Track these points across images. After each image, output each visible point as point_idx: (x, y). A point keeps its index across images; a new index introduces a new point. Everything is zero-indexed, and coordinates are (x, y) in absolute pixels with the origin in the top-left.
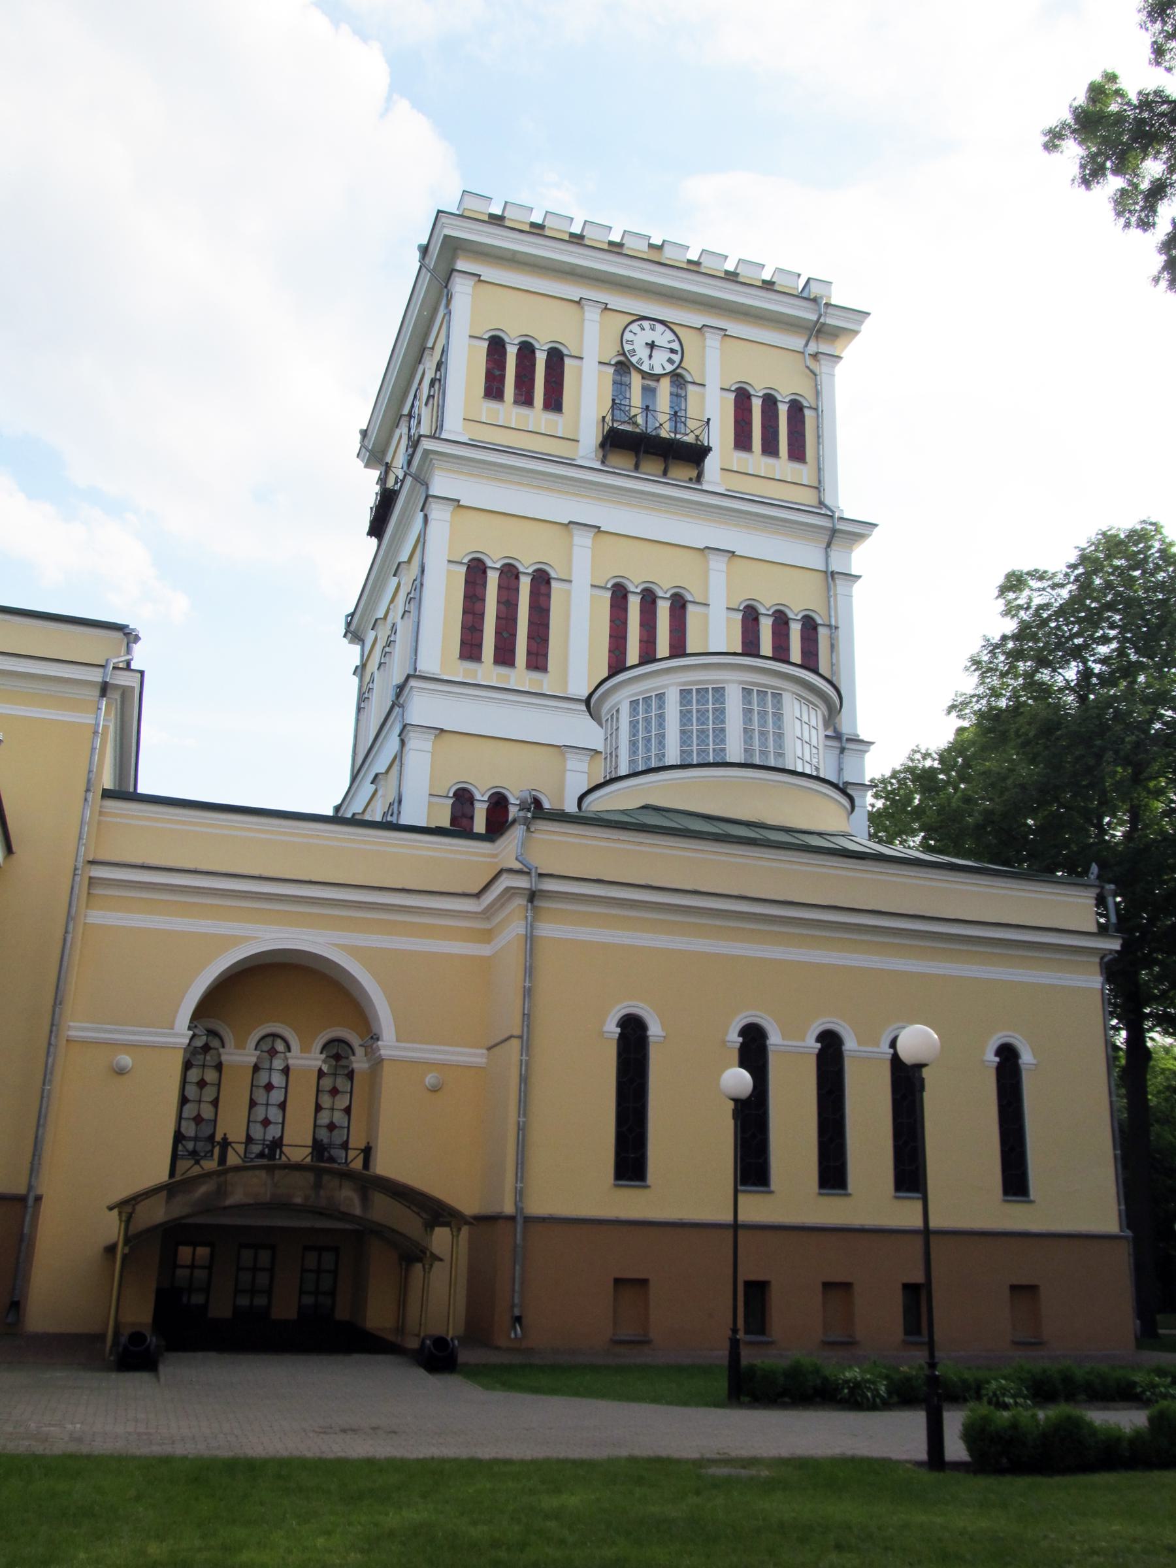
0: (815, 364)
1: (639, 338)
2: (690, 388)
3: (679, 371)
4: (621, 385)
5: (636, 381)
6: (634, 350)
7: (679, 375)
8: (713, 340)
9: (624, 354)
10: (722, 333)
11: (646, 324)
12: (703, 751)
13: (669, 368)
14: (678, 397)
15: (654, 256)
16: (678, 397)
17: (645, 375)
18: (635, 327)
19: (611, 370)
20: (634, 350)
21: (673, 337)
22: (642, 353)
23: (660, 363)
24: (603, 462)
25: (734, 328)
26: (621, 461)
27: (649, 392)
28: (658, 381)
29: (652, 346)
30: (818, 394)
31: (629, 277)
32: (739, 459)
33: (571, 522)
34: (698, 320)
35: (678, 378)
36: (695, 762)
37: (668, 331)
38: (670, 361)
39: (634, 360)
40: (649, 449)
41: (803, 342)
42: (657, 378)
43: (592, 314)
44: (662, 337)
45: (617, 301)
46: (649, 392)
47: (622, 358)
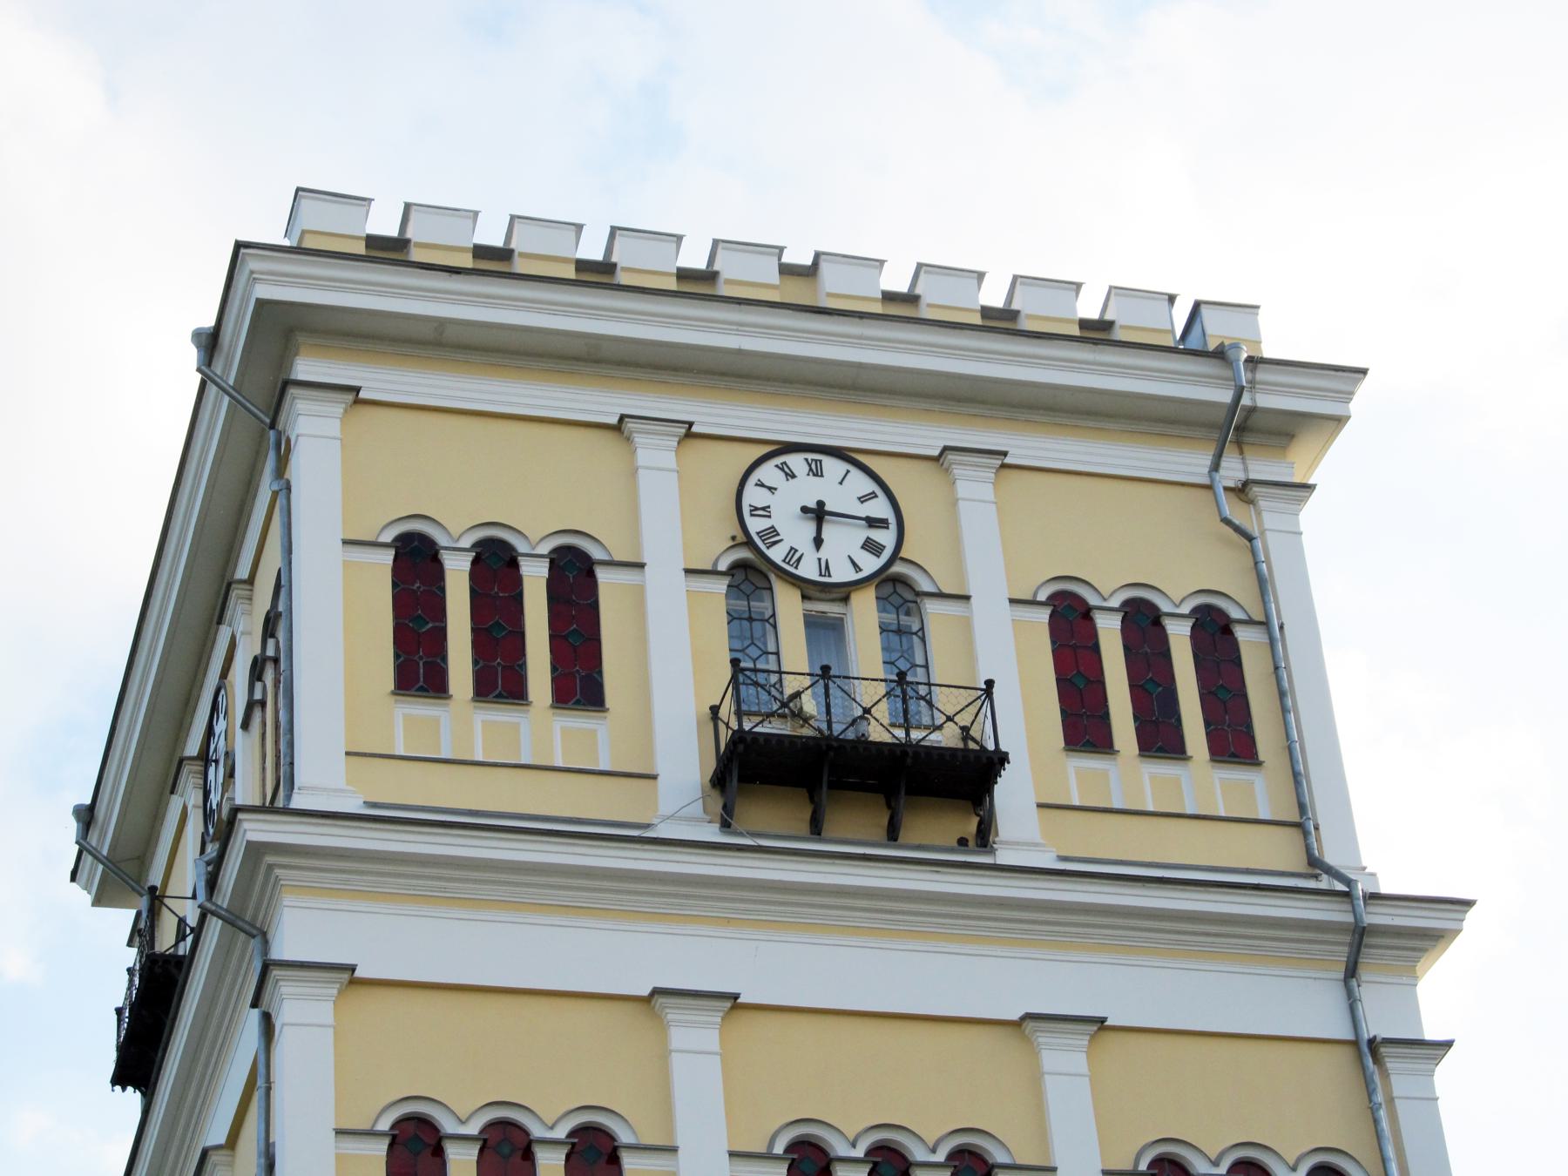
0: (1244, 514)
1: (783, 499)
2: (931, 607)
3: (898, 568)
6: (773, 531)
7: (900, 581)
11: (796, 461)
13: (871, 564)
15: (796, 292)
16: (902, 634)
17: (809, 590)
18: (769, 472)
19: (720, 586)
20: (773, 531)
21: (869, 486)
22: (797, 534)
23: (844, 557)
24: (726, 825)
25: (1025, 446)
26: (777, 815)
27: (826, 631)
28: (845, 599)
29: (818, 514)
30: (1263, 584)
31: (740, 352)
32: (1081, 776)
33: (656, 992)
34: (928, 436)
35: (895, 588)
37: (856, 475)
38: (871, 547)
39: (777, 554)
40: (844, 777)
41: (1206, 460)
42: (843, 592)
43: (656, 455)
46: (826, 631)
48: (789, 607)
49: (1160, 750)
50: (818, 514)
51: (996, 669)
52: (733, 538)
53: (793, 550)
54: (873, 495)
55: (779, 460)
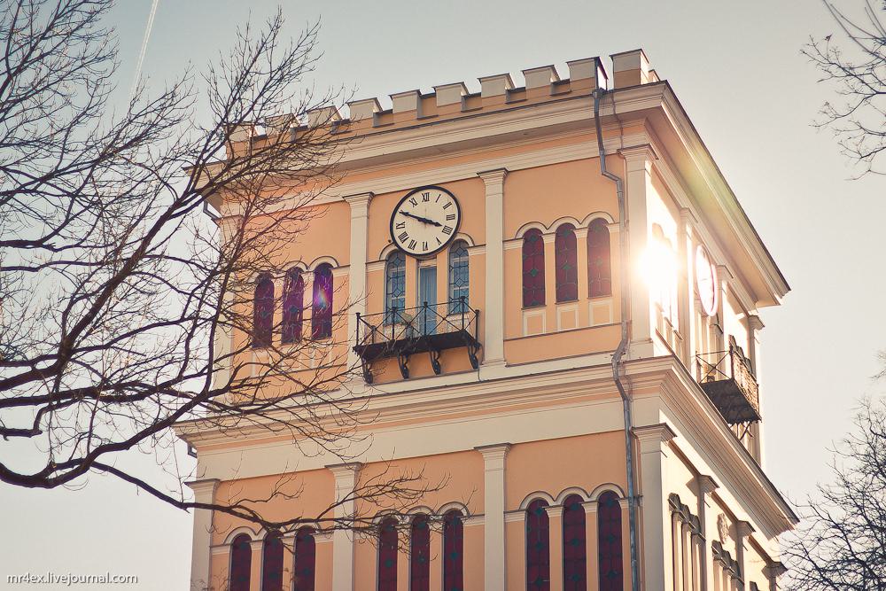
2: (471, 252)
3: (458, 237)
4: (395, 280)
5: (410, 267)
6: (405, 234)
8: (494, 186)
11: (418, 197)
13: (445, 238)
14: (459, 272)
19: (382, 266)
20: (405, 234)
25: (513, 161)
26: (392, 368)
27: (427, 275)
34: (468, 169)
37: (443, 194)
39: (405, 246)
40: (423, 348)
43: (359, 209)
44: (436, 207)
45: (380, 185)
46: (427, 275)
52: (390, 241)
54: (450, 204)
55: (410, 199)
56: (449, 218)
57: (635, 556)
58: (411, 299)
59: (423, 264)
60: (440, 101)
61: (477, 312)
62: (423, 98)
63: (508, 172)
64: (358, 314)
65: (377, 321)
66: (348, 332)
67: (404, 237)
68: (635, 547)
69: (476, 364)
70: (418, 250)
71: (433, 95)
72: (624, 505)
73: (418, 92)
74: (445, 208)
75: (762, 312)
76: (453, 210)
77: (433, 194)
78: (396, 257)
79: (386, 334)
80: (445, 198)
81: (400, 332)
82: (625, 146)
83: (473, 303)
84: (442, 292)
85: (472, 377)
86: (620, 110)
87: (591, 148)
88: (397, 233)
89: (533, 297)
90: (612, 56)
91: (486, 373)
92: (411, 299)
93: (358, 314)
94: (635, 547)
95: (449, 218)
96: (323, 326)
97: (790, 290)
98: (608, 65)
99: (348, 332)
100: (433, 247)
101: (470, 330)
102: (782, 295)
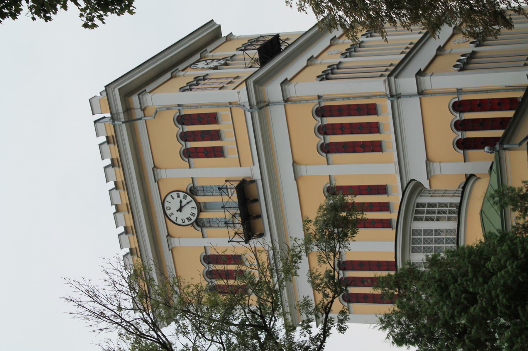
1: (179, 217)
3: (188, 191)
5: (204, 215)
6: (188, 219)
8: (162, 174)
9: (192, 224)
10: (155, 169)
11: (168, 212)
12: (446, 240)
13: (189, 198)
14: (205, 191)
17: (200, 211)
18: (173, 218)
19: (205, 230)
20: (188, 219)
31: (147, 230)
35: (193, 192)
36: (456, 237)
37: (167, 199)
38: (185, 198)
39: (194, 218)
43: (176, 242)
44: (173, 204)
45: (163, 233)
47: (195, 224)
48: (204, 215)
49: (215, 118)
50: (180, 210)
51: (209, 172)
53: (191, 215)
56: (178, 196)
57: (348, 98)
58: (219, 215)
59: (203, 210)
60: (119, 202)
61: (226, 181)
62: (118, 210)
63: (155, 166)
64: (229, 242)
65: (232, 232)
66: (239, 247)
67: (189, 219)
68: (343, 99)
69: (253, 182)
70: (196, 211)
71: (117, 206)
72: (323, 104)
73: (114, 213)
74: (173, 198)
75: (224, 33)
76: (174, 195)
77: (167, 204)
78: (199, 223)
79: (240, 228)
80: (169, 198)
81: (238, 220)
82: (139, 107)
83: (222, 183)
84: (217, 199)
85: (260, 183)
86: (120, 110)
87: (141, 125)
88: (187, 222)
89: (218, 152)
90: (93, 114)
91: (257, 176)
92: (219, 215)
93: (229, 242)
94: (343, 99)
95: (178, 196)
96: (237, 259)
97: (212, 20)
98: (98, 116)
99: (239, 247)
100: (193, 204)
101: (235, 184)
102: (215, 24)
